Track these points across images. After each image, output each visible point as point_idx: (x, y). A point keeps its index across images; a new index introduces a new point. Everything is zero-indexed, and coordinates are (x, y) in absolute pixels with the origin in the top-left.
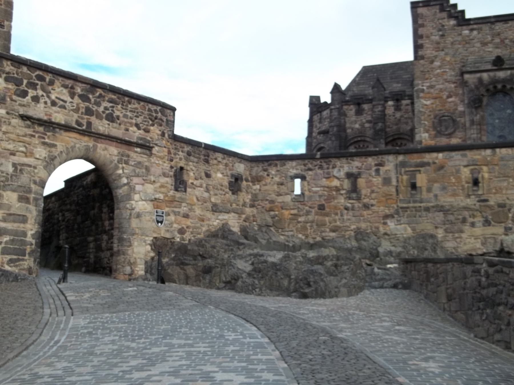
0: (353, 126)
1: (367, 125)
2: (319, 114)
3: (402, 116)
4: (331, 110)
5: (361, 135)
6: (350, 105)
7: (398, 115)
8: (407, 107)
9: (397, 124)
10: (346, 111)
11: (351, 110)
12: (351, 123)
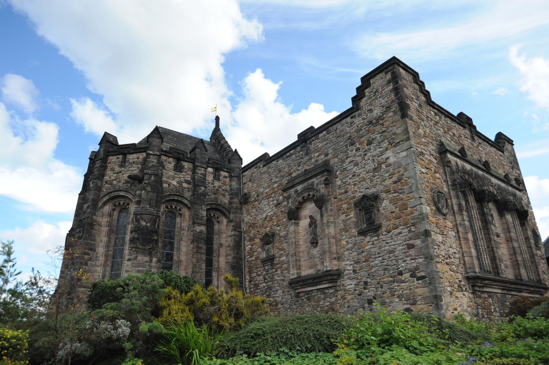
0: (170, 181)
1: (185, 185)
2: (121, 156)
3: (220, 187)
4: (148, 154)
5: (178, 194)
6: (169, 157)
7: (217, 184)
8: (225, 179)
9: (215, 194)
10: (164, 162)
11: (170, 164)
12: (169, 177)
